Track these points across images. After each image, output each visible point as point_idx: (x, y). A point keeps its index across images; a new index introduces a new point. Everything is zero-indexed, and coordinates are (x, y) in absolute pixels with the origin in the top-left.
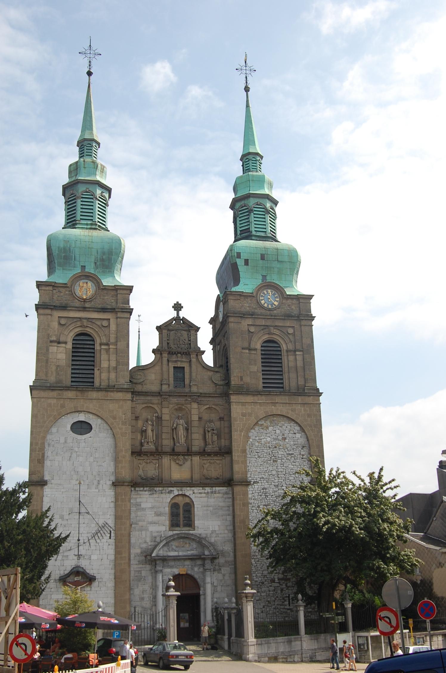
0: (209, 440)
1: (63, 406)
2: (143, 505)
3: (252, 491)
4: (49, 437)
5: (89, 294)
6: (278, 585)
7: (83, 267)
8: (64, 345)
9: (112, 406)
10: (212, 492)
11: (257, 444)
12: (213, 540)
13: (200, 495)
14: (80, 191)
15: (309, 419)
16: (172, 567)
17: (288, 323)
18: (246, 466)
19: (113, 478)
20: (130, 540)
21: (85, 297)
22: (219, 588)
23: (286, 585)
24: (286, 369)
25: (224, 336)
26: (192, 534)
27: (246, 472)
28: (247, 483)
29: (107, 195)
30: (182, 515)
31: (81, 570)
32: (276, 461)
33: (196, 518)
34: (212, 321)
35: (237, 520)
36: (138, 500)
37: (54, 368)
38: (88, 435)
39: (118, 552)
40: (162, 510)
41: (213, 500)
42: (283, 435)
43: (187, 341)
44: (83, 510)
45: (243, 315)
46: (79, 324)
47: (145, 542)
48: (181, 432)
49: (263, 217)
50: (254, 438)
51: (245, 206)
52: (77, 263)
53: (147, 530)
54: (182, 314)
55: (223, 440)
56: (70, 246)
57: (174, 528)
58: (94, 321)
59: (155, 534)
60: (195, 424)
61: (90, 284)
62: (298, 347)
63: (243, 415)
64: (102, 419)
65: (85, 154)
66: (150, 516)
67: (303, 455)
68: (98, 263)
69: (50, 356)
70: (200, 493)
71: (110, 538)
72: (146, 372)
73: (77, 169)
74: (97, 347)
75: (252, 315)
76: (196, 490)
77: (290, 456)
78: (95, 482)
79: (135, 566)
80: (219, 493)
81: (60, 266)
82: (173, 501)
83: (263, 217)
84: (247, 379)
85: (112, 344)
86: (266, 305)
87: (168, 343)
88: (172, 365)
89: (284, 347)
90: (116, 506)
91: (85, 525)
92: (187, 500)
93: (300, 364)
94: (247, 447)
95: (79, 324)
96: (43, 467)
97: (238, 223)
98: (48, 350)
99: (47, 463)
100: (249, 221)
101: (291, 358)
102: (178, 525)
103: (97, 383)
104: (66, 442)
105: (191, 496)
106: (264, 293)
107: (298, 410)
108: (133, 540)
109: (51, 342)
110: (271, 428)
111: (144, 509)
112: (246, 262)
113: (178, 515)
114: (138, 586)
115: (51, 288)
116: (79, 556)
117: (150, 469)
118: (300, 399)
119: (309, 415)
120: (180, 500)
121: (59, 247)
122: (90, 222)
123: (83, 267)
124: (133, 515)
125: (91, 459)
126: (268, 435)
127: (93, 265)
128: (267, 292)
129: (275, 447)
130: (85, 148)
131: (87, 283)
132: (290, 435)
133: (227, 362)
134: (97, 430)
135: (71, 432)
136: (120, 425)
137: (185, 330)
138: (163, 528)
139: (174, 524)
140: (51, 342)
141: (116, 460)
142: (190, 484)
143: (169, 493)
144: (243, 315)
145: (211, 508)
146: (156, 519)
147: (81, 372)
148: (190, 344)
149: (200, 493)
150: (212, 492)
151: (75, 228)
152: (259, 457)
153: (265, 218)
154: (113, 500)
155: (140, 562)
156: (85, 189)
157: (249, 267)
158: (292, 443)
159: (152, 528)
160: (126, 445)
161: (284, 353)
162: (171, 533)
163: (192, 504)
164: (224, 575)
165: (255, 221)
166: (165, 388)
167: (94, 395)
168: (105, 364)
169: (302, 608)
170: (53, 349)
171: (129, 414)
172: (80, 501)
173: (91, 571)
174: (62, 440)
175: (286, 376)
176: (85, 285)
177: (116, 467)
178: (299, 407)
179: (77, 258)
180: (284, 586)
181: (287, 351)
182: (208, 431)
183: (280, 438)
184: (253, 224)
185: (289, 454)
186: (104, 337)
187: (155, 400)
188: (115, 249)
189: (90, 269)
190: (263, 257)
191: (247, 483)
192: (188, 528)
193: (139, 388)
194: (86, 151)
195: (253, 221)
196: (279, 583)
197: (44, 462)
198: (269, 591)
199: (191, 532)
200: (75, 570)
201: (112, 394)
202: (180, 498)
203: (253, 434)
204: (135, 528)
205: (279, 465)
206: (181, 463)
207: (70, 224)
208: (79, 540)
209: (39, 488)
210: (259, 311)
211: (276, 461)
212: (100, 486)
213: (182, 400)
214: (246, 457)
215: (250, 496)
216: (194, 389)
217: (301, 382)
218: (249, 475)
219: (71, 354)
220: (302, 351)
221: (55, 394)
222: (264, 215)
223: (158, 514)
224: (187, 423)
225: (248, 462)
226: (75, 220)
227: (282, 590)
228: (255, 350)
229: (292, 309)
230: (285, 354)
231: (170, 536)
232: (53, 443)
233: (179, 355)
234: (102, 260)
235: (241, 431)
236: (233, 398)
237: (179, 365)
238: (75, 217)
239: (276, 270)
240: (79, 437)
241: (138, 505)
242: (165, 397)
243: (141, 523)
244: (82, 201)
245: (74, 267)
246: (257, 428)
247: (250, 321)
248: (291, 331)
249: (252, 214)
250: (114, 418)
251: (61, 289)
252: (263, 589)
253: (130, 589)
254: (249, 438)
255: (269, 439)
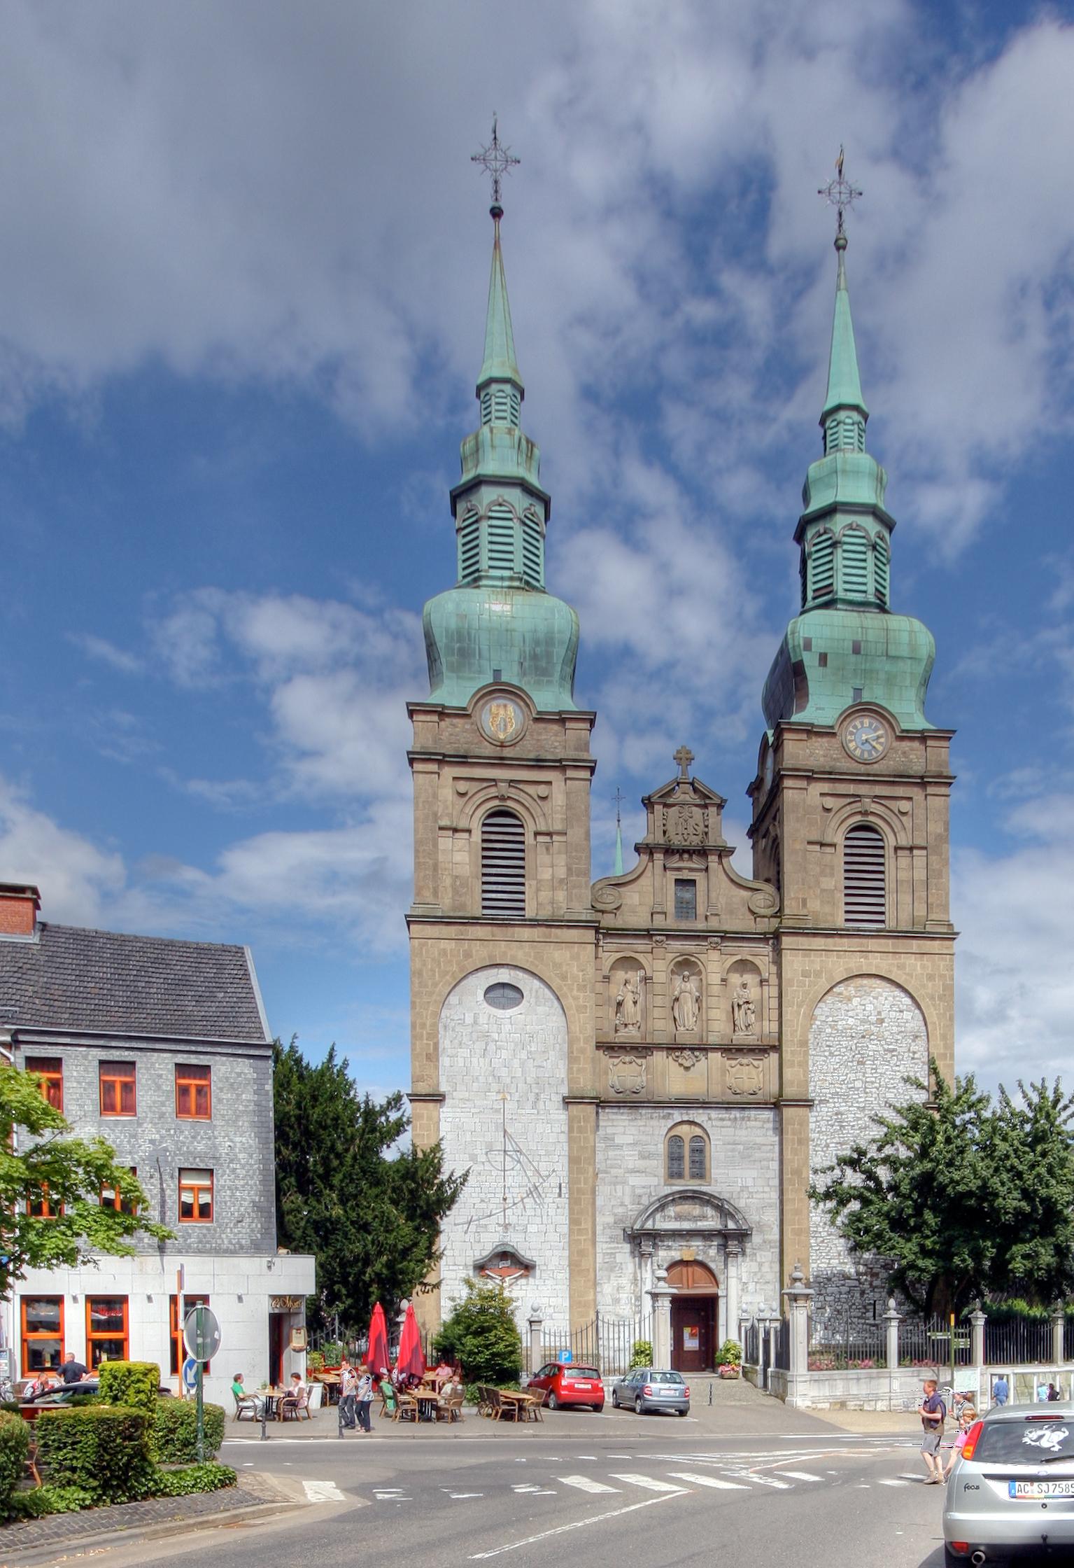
0: (741, 1022)
1: (468, 955)
2: (618, 1140)
3: (816, 1120)
4: (445, 1013)
5: (510, 730)
6: (856, 1283)
7: (497, 673)
8: (466, 835)
9: (558, 954)
10: (743, 1119)
11: (828, 1030)
12: (741, 1204)
13: (720, 1123)
14: (485, 502)
15: (930, 984)
16: (669, 1248)
17: (900, 791)
18: (806, 1072)
19: (565, 1091)
20: (594, 1199)
21: (502, 737)
22: (751, 1287)
23: (871, 1284)
24: (893, 886)
25: (774, 818)
26: (705, 1194)
27: (806, 1083)
28: (807, 1104)
29: (539, 510)
30: (686, 1158)
31: (509, 1249)
32: (863, 1063)
33: (713, 1164)
34: (754, 789)
35: (787, 1168)
36: (609, 1130)
37: (448, 881)
38: (515, 1010)
39: (574, 1221)
40: (652, 1148)
41: (744, 1132)
42: (879, 1013)
43: (701, 829)
44: (509, 1147)
45: (810, 776)
46: (493, 792)
47: (622, 1204)
48: (689, 1006)
49: (862, 556)
50: (823, 1018)
51: (825, 533)
52: (485, 663)
53: (624, 1183)
54: (694, 772)
55: (766, 1023)
56: (469, 628)
57: (674, 1181)
58: (520, 786)
59: (638, 1191)
60: (715, 990)
61: (511, 708)
62: (920, 842)
63: (805, 974)
64: (541, 979)
65: (494, 414)
66: (631, 1159)
67: (914, 1053)
68: (526, 664)
69: (441, 858)
70: (722, 1119)
71: (560, 1195)
72: (622, 889)
73: (477, 450)
74: (529, 839)
75: (831, 776)
76: (714, 1114)
77: (889, 1055)
78: (532, 1097)
79: (605, 1246)
80: (756, 1120)
81: (453, 671)
82: (672, 1133)
83: (862, 556)
84: (814, 905)
85: (559, 833)
86: (858, 753)
87: (665, 832)
88: (672, 876)
89: (890, 841)
90: (571, 1140)
91: (514, 1173)
92: (698, 1131)
93: (920, 874)
94: (810, 1036)
95: (493, 792)
96: (437, 1068)
97: (810, 572)
98: (435, 845)
99: (444, 1061)
100: (831, 569)
101: (904, 861)
102: (680, 1175)
103: (529, 913)
104: (475, 1022)
105: (704, 1125)
106: (855, 727)
107: (912, 964)
108: (599, 1201)
109: (441, 828)
110: (856, 1001)
111: (620, 1147)
112: (823, 659)
113: (680, 1158)
114: (609, 1279)
115: (435, 718)
116: (506, 1226)
117: (624, 1074)
118: (915, 945)
119: (931, 977)
120: (684, 1131)
121: (447, 631)
122: (507, 573)
123: (497, 673)
124: (599, 1156)
125: (524, 1055)
126: (850, 1014)
127: (516, 668)
128: (862, 723)
129: (863, 1037)
130: (494, 400)
131: (505, 706)
132: (893, 1014)
133: (778, 873)
134: (533, 1000)
135: (485, 1005)
136: (575, 993)
137: (696, 805)
138: (654, 1181)
139: (674, 1174)
140: (441, 828)
141: (572, 1059)
142: (705, 1105)
143: (664, 1117)
144: (810, 776)
145: (741, 1147)
146: (641, 1164)
147: (500, 888)
148: (706, 833)
149: (722, 1119)
150: (743, 1119)
151: (478, 587)
152: (832, 1054)
153: (864, 560)
154: (565, 1128)
155: (612, 1239)
156: (494, 497)
157: (828, 670)
158: (895, 1029)
159: (634, 1180)
160: (587, 1032)
161: (889, 852)
162: (668, 1190)
163: (705, 1137)
164: (761, 1265)
165: (845, 566)
166: (659, 922)
167: (526, 933)
168: (546, 874)
169: (895, 1323)
170: (446, 842)
171: (590, 970)
172: (505, 1131)
173: (526, 1253)
174: (469, 1019)
175: (889, 900)
176: (502, 712)
177: (570, 1070)
178: (911, 960)
179: (485, 653)
180: (866, 1286)
181: (896, 849)
182: (739, 1006)
183: (873, 1018)
184: (840, 582)
185: (888, 1050)
186: (541, 819)
187: (641, 944)
188: (560, 632)
189: (510, 676)
190: (856, 650)
191: (807, 1104)
192: (699, 1182)
193: (607, 921)
194: (494, 407)
195: (840, 566)
196: (858, 1280)
197: (438, 1060)
198: (840, 1293)
199: (704, 1189)
200: (499, 1249)
201: (558, 931)
202: (685, 1128)
203: (823, 1010)
204: (603, 1179)
205: (869, 1071)
206: (687, 1064)
207: (469, 579)
208: (505, 1199)
209: (431, 1105)
210: (845, 765)
211: (863, 1063)
212: (541, 1103)
213: (689, 946)
214: (806, 1053)
215: (812, 1126)
216: (714, 924)
217: (921, 911)
218: (811, 1089)
219: (481, 854)
220: (925, 848)
221: (452, 931)
222: (864, 553)
223: (643, 1156)
224: (700, 989)
225: (810, 1063)
226: (477, 570)
227: (863, 1293)
228: (834, 845)
229: (911, 761)
230: (892, 851)
231: (667, 1196)
232: (452, 1024)
233: (686, 856)
234: (535, 657)
235: (799, 1006)
236: (787, 941)
237: (686, 875)
238: (477, 562)
239: (882, 676)
240: (499, 1013)
241: (609, 1139)
242: (658, 938)
243: (614, 1171)
244: (491, 526)
245: (480, 672)
246: (829, 998)
247: (826, 787)
248: (905, 806)
249: (839, 550)
250: (564, 978)
251: (456, 721)
252: (829, 1290)
253: (595, 1284)
254: (812, 1017)
255: (851, 1022)
